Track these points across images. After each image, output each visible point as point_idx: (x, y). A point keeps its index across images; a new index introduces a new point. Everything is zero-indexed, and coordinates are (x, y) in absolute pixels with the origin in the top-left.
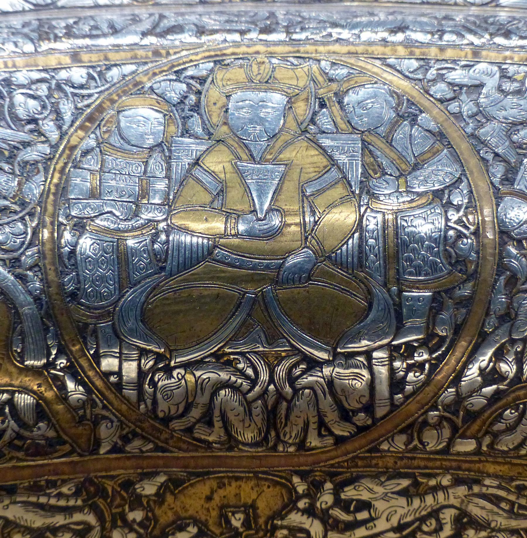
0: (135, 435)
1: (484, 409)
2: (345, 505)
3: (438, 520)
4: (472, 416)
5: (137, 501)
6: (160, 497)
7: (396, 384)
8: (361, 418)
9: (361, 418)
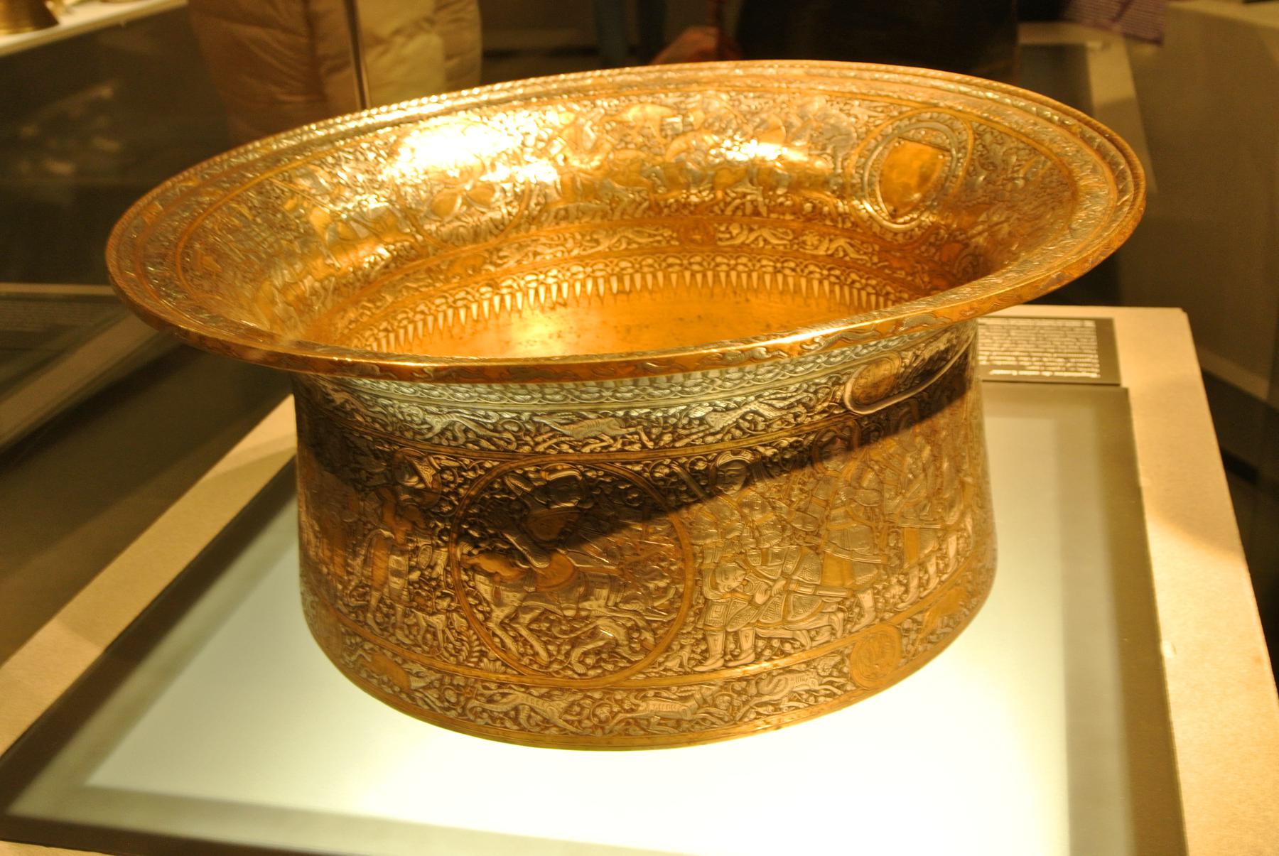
2: (500, 258)
4: (534, 219)
5: (441, 272)
6: (448, 270)
7: (509, 214)
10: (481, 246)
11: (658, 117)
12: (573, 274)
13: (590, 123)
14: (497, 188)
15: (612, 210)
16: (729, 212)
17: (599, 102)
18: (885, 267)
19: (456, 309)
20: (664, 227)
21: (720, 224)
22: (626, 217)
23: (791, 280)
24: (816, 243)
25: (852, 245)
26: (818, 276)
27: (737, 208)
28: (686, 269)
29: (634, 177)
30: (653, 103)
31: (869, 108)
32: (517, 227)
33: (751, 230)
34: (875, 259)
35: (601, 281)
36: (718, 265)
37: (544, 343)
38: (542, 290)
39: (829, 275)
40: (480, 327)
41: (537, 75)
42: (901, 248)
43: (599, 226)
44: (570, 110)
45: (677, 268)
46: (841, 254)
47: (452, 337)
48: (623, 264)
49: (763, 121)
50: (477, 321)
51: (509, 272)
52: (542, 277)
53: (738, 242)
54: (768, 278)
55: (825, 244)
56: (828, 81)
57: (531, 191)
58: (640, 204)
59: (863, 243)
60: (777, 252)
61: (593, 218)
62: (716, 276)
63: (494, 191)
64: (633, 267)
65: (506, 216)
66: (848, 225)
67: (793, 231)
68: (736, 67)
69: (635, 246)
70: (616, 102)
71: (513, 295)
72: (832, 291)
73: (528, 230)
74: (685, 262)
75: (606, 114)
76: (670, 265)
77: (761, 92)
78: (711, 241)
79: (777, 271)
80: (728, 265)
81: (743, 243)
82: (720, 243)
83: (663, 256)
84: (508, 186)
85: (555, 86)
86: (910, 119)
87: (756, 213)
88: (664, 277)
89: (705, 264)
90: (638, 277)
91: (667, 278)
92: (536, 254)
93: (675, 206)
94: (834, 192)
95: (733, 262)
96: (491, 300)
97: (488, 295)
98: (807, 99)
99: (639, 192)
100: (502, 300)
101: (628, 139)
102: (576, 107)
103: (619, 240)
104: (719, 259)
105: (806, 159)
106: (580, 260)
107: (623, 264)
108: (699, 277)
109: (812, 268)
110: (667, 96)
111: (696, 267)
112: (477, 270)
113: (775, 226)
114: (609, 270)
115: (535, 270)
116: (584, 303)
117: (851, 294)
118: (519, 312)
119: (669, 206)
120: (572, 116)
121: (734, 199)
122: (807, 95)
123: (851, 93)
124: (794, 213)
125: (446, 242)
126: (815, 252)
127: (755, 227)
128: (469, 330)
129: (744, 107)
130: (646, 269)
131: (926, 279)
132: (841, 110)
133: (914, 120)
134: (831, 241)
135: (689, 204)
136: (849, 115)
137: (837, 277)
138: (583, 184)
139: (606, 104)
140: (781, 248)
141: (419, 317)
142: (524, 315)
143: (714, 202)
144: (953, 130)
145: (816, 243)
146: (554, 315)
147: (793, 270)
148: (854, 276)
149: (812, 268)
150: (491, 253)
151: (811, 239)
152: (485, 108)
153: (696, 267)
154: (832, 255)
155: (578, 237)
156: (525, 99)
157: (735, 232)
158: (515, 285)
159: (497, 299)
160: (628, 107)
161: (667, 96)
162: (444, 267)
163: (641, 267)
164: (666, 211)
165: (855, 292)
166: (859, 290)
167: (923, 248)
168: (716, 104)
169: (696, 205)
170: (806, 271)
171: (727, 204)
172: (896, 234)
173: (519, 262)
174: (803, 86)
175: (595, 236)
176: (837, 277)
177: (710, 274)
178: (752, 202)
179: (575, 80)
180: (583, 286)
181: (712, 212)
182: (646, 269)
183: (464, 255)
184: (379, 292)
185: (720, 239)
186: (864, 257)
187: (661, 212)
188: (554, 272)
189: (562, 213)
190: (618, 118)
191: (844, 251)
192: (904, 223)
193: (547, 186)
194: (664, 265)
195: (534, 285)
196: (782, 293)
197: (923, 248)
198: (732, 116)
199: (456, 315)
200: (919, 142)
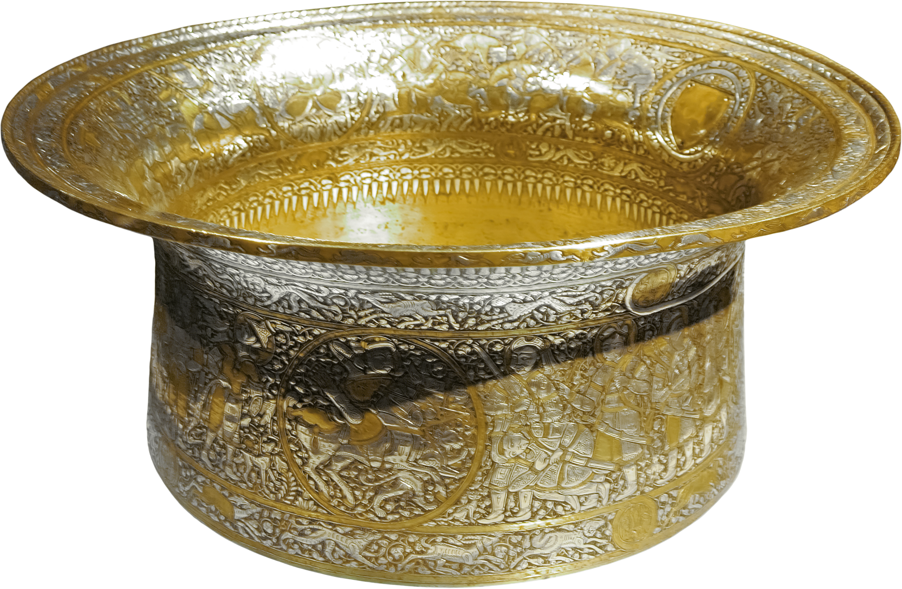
2: (342, 156)
4: (373, 124)
5: (290, 163)
6: (296, 162)
7: (352, 118)
8: (344, 129)
10: (326, 144)
11: (486, 46)
12: (403, 175)
13: (427, 46)
14: (343, 96)
15: (440, 122)
16: (540, 132)
17: (436, 29)
18: (670, 190)
19: (300, 197)
20: (484, 141)
21: (532, 143)
23: (588, 195)
24: (612, 165)
25: (643, 170)
26: (611, 193)
27: (547, 130)
28: (500, 178)
29: (461, 96)
30: (482, 33)
31: (668, 53)
32: (358, 131)
33: (558, 150)
34: (662, 183)
35: (426, 183)
36: (527, 177)
37: (372, 231)
38: (375, 186)
39: (621, 194)
40: (319, 213)
42: (685, 175)
43: (428, 136)
44: (412, 34)
45: (492, 177)
46: (633, 177)
47: (294, 220)
48: (446, 170)
50: (317, 208)
51: (347, 168)
52: (375, 175)
53: (546, 159)
54: (568, 192)
55: (620, 167)
56: (635, 26)
57: (372, 101)
58: (465, 119)
59: (653, 168)
60: (579, 170)
61: (424, 128)
62: (525, 187)
63: (340, 98)
64: (454, 173)
65: (349, 120)
66: (642, 152)
67: (594, 154)
68: (557, 8)
69: (457, 155)
70: (451, 30)
71: (350, 189)
72: (623, 208)
73: (367, 134)
74: (499, 172)
75: (442, 40)
76: (486, 174)
77: (576, 30)
79: (577, 186)
80: (536, 178)
81: (550, 160)
82: (530, 159)
83: (481, 166)
84: (353, 95)
85: (400, 12)
86: (702, 65)
87: (563, 135)
88: (480, 184)
89: (516, 175)
90: (457, 182)
91: (482, 184)
92: (372, 155)
93: (494, 124)
94: (631, 122)
95: (540, 176)
96: (330, 191)
97: (328, 187)
98: (616, 41)
99: (465, 109)
100: (340, 192)
101: (459, 63)
102: (416, 31)
103: (444, 149)
104: (528, 173)
105: (610, 92)
106: (409, 163)
107: (446, 170)
108: (510, 186)
109: (607, 186)
110: (495, 28)
111: (508, 178)
112: (320, 164)
113: (578, 148)
114: (433, 174)
115: (370, 168)
116: (410, 200)
117: (639, 211)
118: (354, 203)
119: (489, 124)
120: (412, 39)
121: (545, 122)
122: (615, 37)
123: (653, 38)
124: (595, 138)
125: (296, 138)
126: (611, 173)
127: (562, 147)
128: (309, 215)
129: (560, 44)
130: (465, 176)
131: (705, 204)
132: (643, 53)
133: (705, 66)
134: (625, 164)
135: (507, 123)
136: (650, 57)
137: (628, 196)
138: (417, 98)
139: (442, 31)
140: (582, 167)
141: (267, 200)
142: (357, 206)
143: (528, 123)
144: (739, 78)
145: (612, 165)
146: (383, 209)
147: (591, 187)
148: (642, 196)
149: (607, 186)
150: (334, 151)
151: (608, 161)
152: (338, 26)
153: (508, 178)
154: (625, 177)
155: (410, 143)
156: (374, 21)
157: (544, 150)
158: (352, 180)
159: (335, 191)
160: (461, 35)
161: (495, 28)
162: (292, 160)
163: (461, 173)
164: (486, 127)
165: (642, 210)
166: (646, 209)
167: (704, 177)
168: (536, 39)
169: (513, 124)
170: (602, 189)
171: (539, 126)
172: (681, 163)
173: (357, 161)
174: (613, 30)
175: (424, 144)
176: (628, 196)
177: (519, 184)
178: (561, 125)
179: (417, 8)
180: (411, 185)
181: (525, 131)
182: (465, 176)
183: (310, 151)
184: (235, 176)
185: (531, 155)
186: (653, 181)
187: (482, 127)
188: (386, 172)
189: (398, 121)
190: (452, 44)
191: (636, 174)
192: (689, 154)
193: (386, 98)
194: (481, 173)
195: (368, 181)
196: (580, 205)
197: (704, 177)
198: (549, 50)
199: (299, 201)
200: (708, 85)
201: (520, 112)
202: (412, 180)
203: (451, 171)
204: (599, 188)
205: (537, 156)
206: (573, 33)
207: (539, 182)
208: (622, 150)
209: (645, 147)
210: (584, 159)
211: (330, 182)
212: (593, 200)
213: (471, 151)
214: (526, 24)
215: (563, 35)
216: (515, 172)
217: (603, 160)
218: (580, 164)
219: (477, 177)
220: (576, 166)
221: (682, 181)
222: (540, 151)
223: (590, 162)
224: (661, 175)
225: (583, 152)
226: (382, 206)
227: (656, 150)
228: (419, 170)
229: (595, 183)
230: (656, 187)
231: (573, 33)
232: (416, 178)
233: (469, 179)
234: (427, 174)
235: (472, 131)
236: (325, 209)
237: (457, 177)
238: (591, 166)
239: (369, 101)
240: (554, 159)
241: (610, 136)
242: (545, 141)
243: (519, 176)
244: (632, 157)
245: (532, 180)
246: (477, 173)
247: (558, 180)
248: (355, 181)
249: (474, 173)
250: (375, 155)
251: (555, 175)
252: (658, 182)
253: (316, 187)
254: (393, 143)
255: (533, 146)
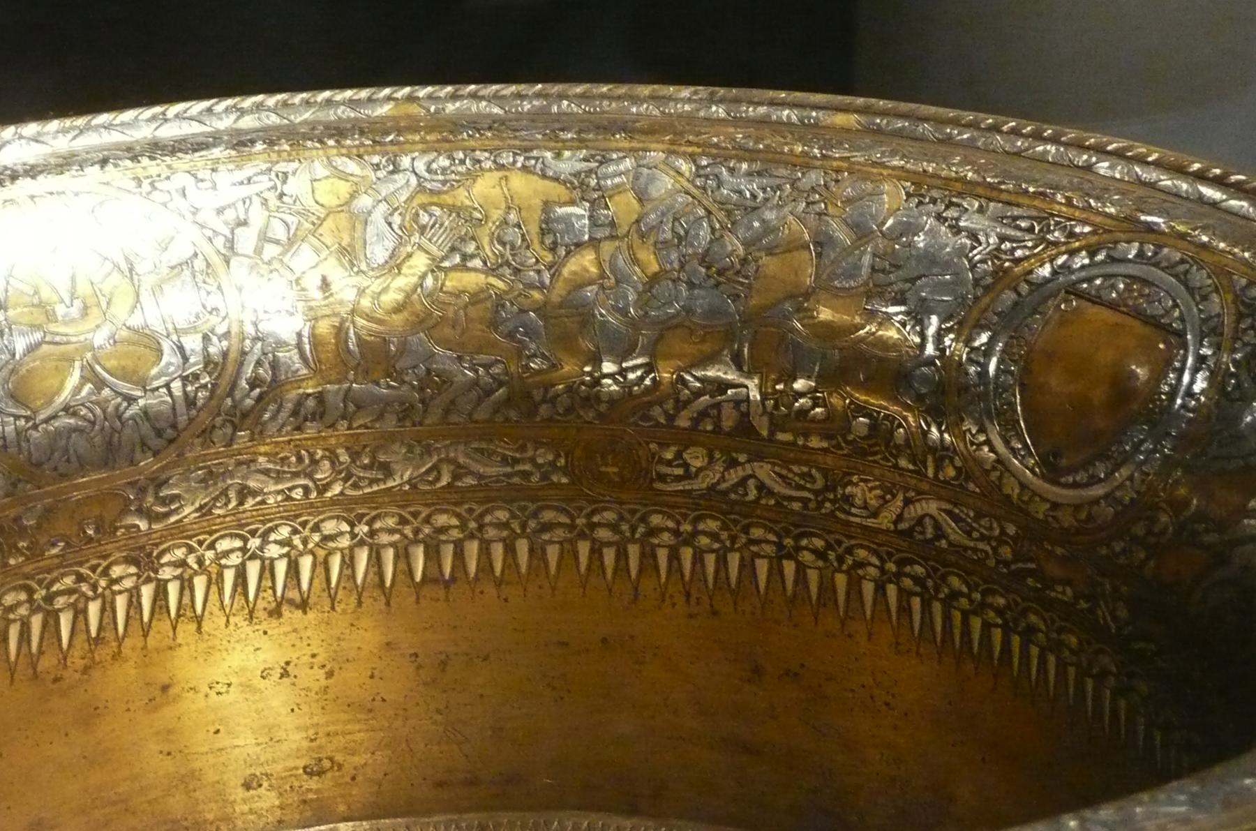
0: (20, 481)
1: (253, 407)
2: (165, 501)
3: (227, 496)
4: (245, 415)
5: (22, 532)
6: (39, 526)
8: (170, 433)
9: (170, 433)
10: (120, 476)
11: (537, 202)
12: (326, 538)
13: (383, 207)
14: (166, 346)
15: (423, 401)
16: (683, 422)
17: (405, 161)
18: (1031, 573)
20: (538, 444)
21: (664, 445)
22: (454, 418)
23: (813, 576)
25: (956, 519)
26: (872, 571)
27: (704, 414)
28: (582, 535)
29: (478, 330)
30: (525, 168)
31: (999, 219)
32: (206, 434)
33: (733, 463)
34: (1006, 552)
35: (389, 555)
36: (653, 532)
37: (247, 687)
38: (253, 569)
40: (103, 653)
41: (271, 90)
43: (391, 438)
44: (343, 176)
45: (560, 534)
46: (930, 532)
47: (36, 675)
48: (442, 520)
49: (768, 229)
50: (98, 640)
51: (179, 531)
53: (700, 484)
54: (762, 567)
56: (909, 146)
57: (244, 353)
58: (489, 393)
59: (979, 516)
61: (381, 417)
62: (648, 556)
63: (160, 352)
64: (463, 527)
65: (181, 407)
66: (951, 472)
67: (825, 473)
68: (712, 100)
69: (470, 481)
70: (444, 162)
71: (186, 585)
72: (905, 610)
73: (231, 441)
74: (580, 521)
75: (421, 189)
76: (547, 527)
77: (765, 163)
78: (640, 482)
79: (782, 554)
80: (676, 533)
81: (712, 488)
82: (659, 486)
83: (532, 507)
84: (193, 343)
85: (307, 115)
86: (1092, 254)
87: (745, 427)
89: (625, 527)
90: (473, 548)
91: (537, 553)
92: (244, 493)
93: (565, 400)
94: (920, 398)
95: (687, 527)
96: (134, 594)
97: (128, 583)
98: (869, 186)
99: (487, 367)
101: (471, 248)
102: (352, 167)
103: (436, 467)
104: (656, 520)
106: (348, 509)
107: (442, 520)
108: (609, 556)
109: (862, 553)
110: (558, 155)
111: (603, 534)
112: (106, 528)
113: (784, 456)
114: (408, 531)
115: (240, 529)
116: (347, 602)
117: (947, 618)
118: (199, 620)
119: (553, 401)
120: (344, 188)
121: (697, 394)
122: (866, 177)
123: (963, 180)
124: (827, 436)
125: (39, 465)
126: (871, 522)
127: (742, 458)
128: (76, 660)
130: (491, 533)
131: (1123, 613)
132: (939, 217)
133: (1100, 257)
134: (908, 502)
135: (598, 398)
136: (957, 230)
138: (361, 342)
139: (420, 166)
140: (796, 506)
142: (206, 626)
144: (1191, 290)
145: (874, 503)
146: (272, 625)
148: (955, 582)
149: (862, 553)
150: (143, 491)
152: (145, 161)
153: (603, 534)
154: (908, 533)
155: (344, 458)
156: (241, 142)
158: (191, 560)
159: (147, 592)
160: (471, 176)
161: (558, 155)
163: (481, 527)
164: (544, 410)
165: (957, 616)
166: (965, 615)
167: (1118, 546)
168: (664, 184)
169: (613, 401)
170: (849, 560)
171: (681, 405)
172: (1055, 506)
173: (205, 511)
174: (859, 157)
175: (382, 458)
176: (917, 580)
177: (634, 551)
178: (737, 402)
179: (351, 103)
180: (349, 563)
181: (645, 417)
182: (491, 533)
183: (77, 495)
185: (662, 478)
186: (981, 545)
187: (533, 411)
188: (285, 532)
189: (311, 403)
190: (448, 199)
191: (937, 526)
192: (1075, 485)
193: (281, 344)
194: (532, 524)
195: (235, 559)
196: (792, 601)
197: (1118, 546)
198: (701, 212)
199: (52, 619)
200: (1112, 306)
201: (634, 369)
202: (351, 548)
203: (455, 522)
204: (841, 560)
205: (678, 479)
206: (757, 166)
207: (686, 543)
208: (896, 466)
209: (958, 463)
210: (802, 488)
211: (133, 570)
212: (827, 588)
213: (509, 469)
214: (635, 144)
215: (732, 171)
216: (622, 518)
217: (849, 489)
218: (791, 499)
219: (523, 534)
220: (778, 504)
221: (1059, 551)
222: (686, 466)
223: (817, 493)
224: (1003, 532)
225: (795, 468)
226: (275, 622)
227: (987, 472)
228: (369, 523)
229: (829, 546)
230: (991, 563)
231: (757, 166)
232: (362, 543)
233: (504, 540)
234: (391, 531)
235: (507, 420)
236: (120, 641)
237: (472, 536)
238: (820, 504)
239: (233, 355)
240: (724, 486)
241: (864, 431)
242: (695, 444)
243: (633, 530)
244: (925, 486)
245: (666, 537)
246: (524, 526)
247: (733, 539)
248: (200, 562)
249: (515, 525)
250: (254, 493)
251: (725, 527)
252: (994, 549)
253: (94, 587)
254: (300, 459)
255: (669, 455)
